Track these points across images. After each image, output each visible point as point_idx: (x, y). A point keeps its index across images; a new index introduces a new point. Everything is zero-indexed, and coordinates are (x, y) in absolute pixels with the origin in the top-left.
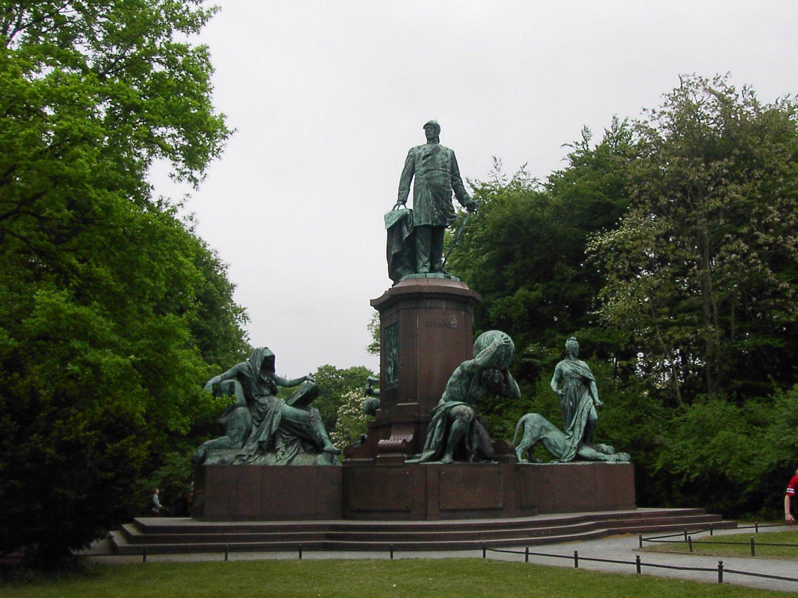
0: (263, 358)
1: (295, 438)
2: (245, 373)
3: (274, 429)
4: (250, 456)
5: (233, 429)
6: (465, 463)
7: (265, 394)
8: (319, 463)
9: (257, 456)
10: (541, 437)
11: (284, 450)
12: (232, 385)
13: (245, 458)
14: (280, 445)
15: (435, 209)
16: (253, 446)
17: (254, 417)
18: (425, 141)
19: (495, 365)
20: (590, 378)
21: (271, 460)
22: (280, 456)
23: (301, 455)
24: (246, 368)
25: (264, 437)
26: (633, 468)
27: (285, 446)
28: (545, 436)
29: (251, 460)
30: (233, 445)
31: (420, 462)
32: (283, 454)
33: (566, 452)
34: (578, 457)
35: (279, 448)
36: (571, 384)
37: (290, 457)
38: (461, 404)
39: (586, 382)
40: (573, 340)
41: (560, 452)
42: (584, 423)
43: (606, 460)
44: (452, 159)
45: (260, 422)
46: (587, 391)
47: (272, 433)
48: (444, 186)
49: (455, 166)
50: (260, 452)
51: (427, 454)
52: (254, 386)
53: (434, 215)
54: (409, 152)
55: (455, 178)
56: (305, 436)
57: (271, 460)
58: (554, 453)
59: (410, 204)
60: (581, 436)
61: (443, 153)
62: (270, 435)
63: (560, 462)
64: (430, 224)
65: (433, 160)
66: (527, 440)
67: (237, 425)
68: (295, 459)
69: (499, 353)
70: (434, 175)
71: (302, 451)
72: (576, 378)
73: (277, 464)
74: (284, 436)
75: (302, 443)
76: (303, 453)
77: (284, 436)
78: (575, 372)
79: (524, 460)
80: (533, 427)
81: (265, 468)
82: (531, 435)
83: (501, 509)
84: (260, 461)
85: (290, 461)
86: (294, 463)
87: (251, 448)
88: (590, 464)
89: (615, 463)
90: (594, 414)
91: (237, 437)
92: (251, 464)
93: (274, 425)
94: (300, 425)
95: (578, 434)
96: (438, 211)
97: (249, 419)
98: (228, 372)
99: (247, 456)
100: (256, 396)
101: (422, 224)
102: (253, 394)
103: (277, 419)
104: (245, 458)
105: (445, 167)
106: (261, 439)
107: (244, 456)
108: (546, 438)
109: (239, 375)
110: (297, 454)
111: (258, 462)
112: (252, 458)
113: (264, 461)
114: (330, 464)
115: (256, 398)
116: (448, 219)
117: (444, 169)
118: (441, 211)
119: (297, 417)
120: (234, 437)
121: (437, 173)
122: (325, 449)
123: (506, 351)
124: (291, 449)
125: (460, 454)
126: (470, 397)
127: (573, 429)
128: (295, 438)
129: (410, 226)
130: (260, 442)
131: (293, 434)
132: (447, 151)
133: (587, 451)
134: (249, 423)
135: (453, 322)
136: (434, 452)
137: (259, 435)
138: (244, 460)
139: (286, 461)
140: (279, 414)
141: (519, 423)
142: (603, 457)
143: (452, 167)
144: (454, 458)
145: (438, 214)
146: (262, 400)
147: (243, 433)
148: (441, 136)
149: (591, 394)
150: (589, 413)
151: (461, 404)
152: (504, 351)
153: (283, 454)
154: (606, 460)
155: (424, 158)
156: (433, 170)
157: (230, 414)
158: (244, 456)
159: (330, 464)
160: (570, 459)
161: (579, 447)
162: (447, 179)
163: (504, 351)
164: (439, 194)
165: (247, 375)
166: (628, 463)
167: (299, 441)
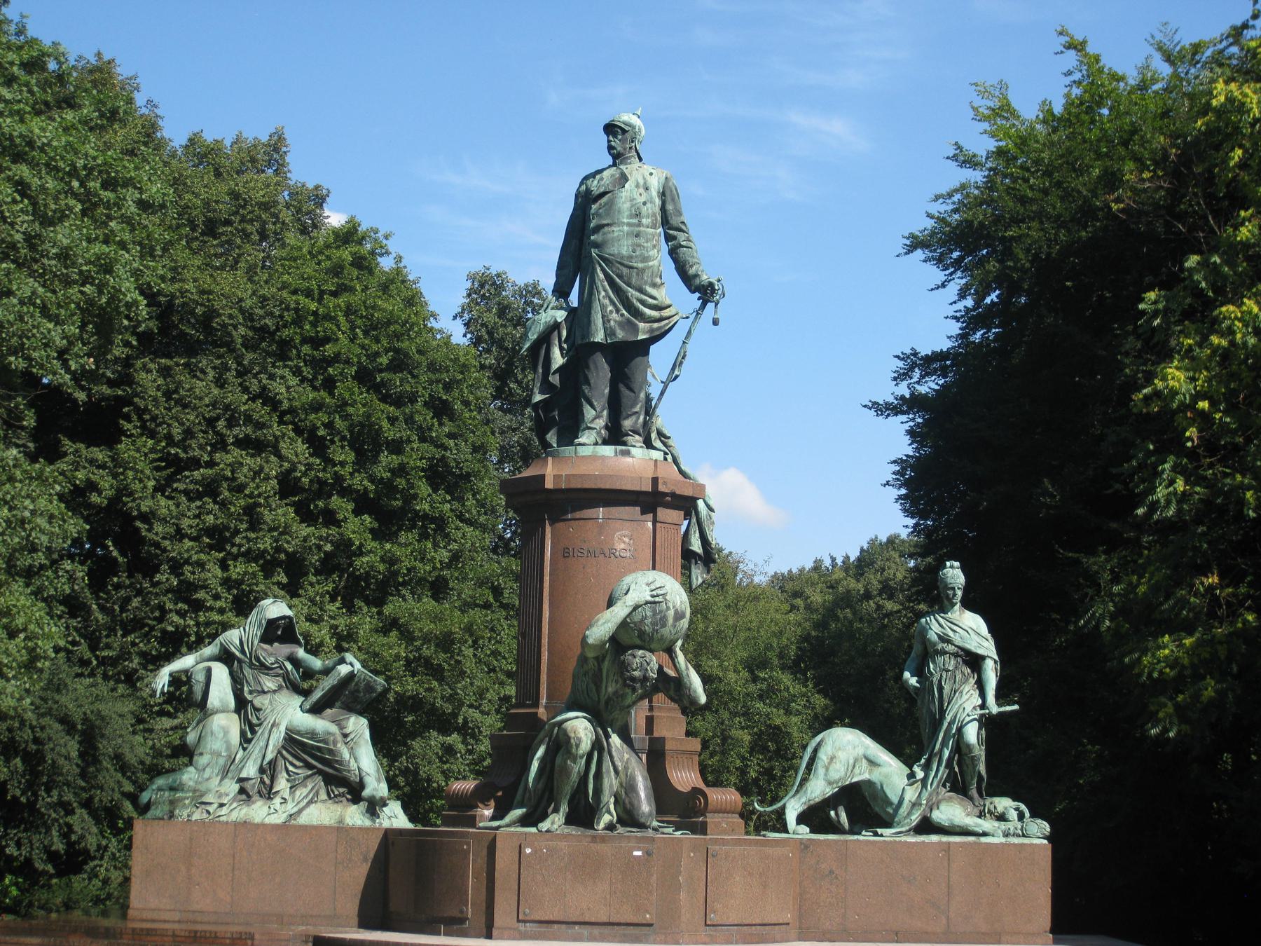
0: (264, 622)
1: (310, 772)
2: (234, 650)
3: (270, 756)
4: (222, 805)
5: (201, 754)
6: (639, 834)
7: (266, 690)
8: (349, 821)
9: (235, 805)
10: (855, 780)
11: (286, 795)
12: (209, 671)
13: (211, 809)
14: (282, 784)
15: (610, 308)
16: (232, 787)
17: (243, 734)
18: (610, 161)
19: (638, 642)
20: (980, 651)
21: (259, 812)
22: (278, 806)
23: (319, 805)
24: (238, 643)
25: (251, 770)
26: (1049, 853)
27: (291, 788)
28: (866, 776)
29: (223, 813)
30: (200, 783)
31: (498, 828)
32: (285, 801)
34: (927, 826)
35: (277, 792)
37: (295, 809)
38: (577, 717)
39: (974, 661)
40: (952, 567)
43: (985, 834)
44: (663, 194)
45: (249, 741)
46: (972, 681)
47: (265, 763)
48: (630, 257)
49: (670, 207)
50: (244, 797)
51: (518, 812)
52: (247, 672)
53: (609, 321)
54: (581, 183)
55: (671, 232)
56: (330, 771)
57: (259, 812)
58: (884, 816)
61: (637, 186)
62: (262, 770)
63: (876, 834)
65: (611, 204)
66: (818, 789)
67: (209, 746)
68: (305, 812)
69: (637, 617)
70: (610, 236)
71: (323, 796)
73: (267, 821)
74: (291, 768)
75: (324, 781)
76: (324, 801)
77: (291, 768)
78: (944, 639)
79: (804, 829)
80: (832, 759)
81: (245, 824)
82: (826, 775)
83: (650, 925)
84: (239, 813)
85: (291, 816)
86: (303, 820)
87: (223, 790)
88: (940, 843)
89: (1003, 840)
90: (972, 733)
91: (208, 771)
92: (221, 819)
93: (270, 747)
94: (319, 749)
96: (618, 311)
97: (235, 737)
98: (209, 650)
99: (215, 806)
100: (251, 692)
102: (246, 689)
103: (278, 737)
104: (211, 809)
105: (638, 215)
106: (243, 775)
107: (210, 804)
108: (869, 783)
109: (225, 657)
110: (311, 802)
111: (234, 816)
112: (225, 808)
113: (245, 814)
114: (367, 823)
115: (249, 697)
116: (642, 325)
117: (635, 221)
118: (624, 312)
119: (312, 734)
120: (204, 770)
121: (616, 231)
122: (366, 793)
123: (654, 614)
124: (301, 792)
125: (582, 815)
126: (607, 703)
128: (310, 772)
130: (241, 780)
131: (308, 766)
132: (648, 177)
134: (233, 743)
135: (623, 546)
136: (524, 810)
137: (242, 769)
138: (208, 812)
139: (285, 815)
140: (283, 729)
141: (809, 750)
142: (978, 825)
143: (663, 209)
144: (569, 821)
145: (617, 319)
146: (258, 701)
147: (222, 761)
150: (960, 730)
151: (577, 717)
152: (648, 614)
153: (285, 801)
154: (985, 834)
156: (608, 225)
157: (201, 726)
158: (210, 804)
159: (367, 823)
160: (907, 828)
162: (641, 241)
163: (648, 614)
164: (620, 277)
165: (237, 653)
166: (1045, 842)
167: (319, 779)
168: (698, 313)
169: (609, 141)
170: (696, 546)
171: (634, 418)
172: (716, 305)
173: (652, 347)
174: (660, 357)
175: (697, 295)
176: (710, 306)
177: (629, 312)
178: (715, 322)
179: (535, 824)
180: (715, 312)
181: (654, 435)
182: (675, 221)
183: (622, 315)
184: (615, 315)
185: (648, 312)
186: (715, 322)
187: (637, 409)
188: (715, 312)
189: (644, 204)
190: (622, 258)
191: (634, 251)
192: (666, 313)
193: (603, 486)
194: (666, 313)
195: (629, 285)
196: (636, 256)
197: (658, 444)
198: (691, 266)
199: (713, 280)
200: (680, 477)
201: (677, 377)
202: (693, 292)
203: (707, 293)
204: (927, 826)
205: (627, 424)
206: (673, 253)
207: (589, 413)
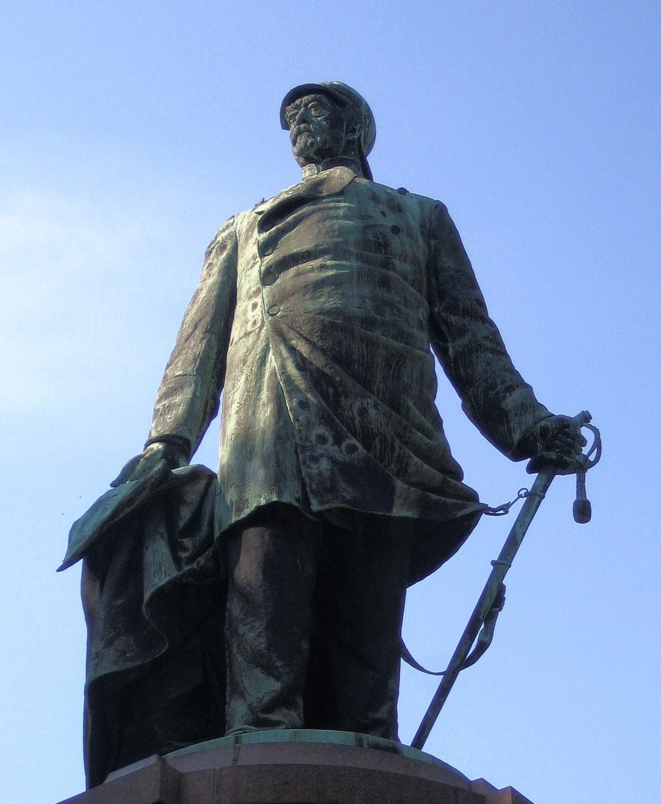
49: (447, 262)
64: (287, 499)
96: (338, 440)
101: (247, 512)
117: (380, 256)
145: (339, 457)
172: (581, 468)
177: (367, 445)
183: (352, 449)
184: (330, 447)
189: (396, 230)
190: (349, 319)
191: (379, 310)
195: (367, 384)
196: (384, 324)
198: (510, 389)
201: (483, 647)
202: (516, 455)
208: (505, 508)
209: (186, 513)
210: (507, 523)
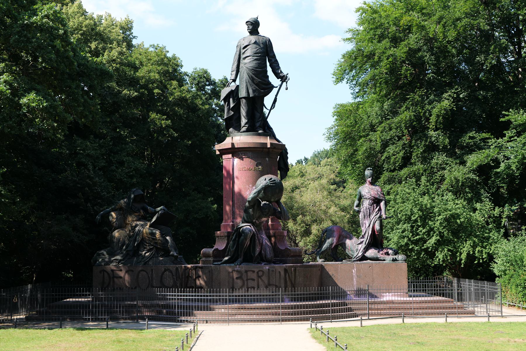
18: (248, 34)
33: (356, 254)
36: (366, 204)
41: (352, 253)
42: (370, 232)
59: (238, 82)
60: (367, 242)
72: (368, 199)
95: (366, 240)
127: (363, 237)
129: (235, 98)
133: (371, 253)
148: (260, 30)
149: (380, 210)
154: (384, 260)
155: (244, 48)
161: (366, 249)
168: (281, 86)
169: (249, 27)
170: (282, 166)
171: (260, 123)
172: (287, 82)
173: (265, 98)
174: (268, 100)
175: (280, 79)
176: (284, 83)
178: (287, 89)
179: (232, 262)
180: (287, 86)
181: (266, 128)
182: (271, 55)
185: (264, 86)
186: (287, 89)
187: (261, 119)
188: (287, 86)
192: (269, 86)
193: (251, 146)
194: (269, 86)
197: (268, 131)
199: (285, 73)
200: (277, 142)
202: (278, 78)
203: (284, 79)
204: (363, 258)
205: (258, 124)
206: (270, 65)
207: (244, 121)
208: (277, 87)
209: (235, 95)
210: (277, 89)
